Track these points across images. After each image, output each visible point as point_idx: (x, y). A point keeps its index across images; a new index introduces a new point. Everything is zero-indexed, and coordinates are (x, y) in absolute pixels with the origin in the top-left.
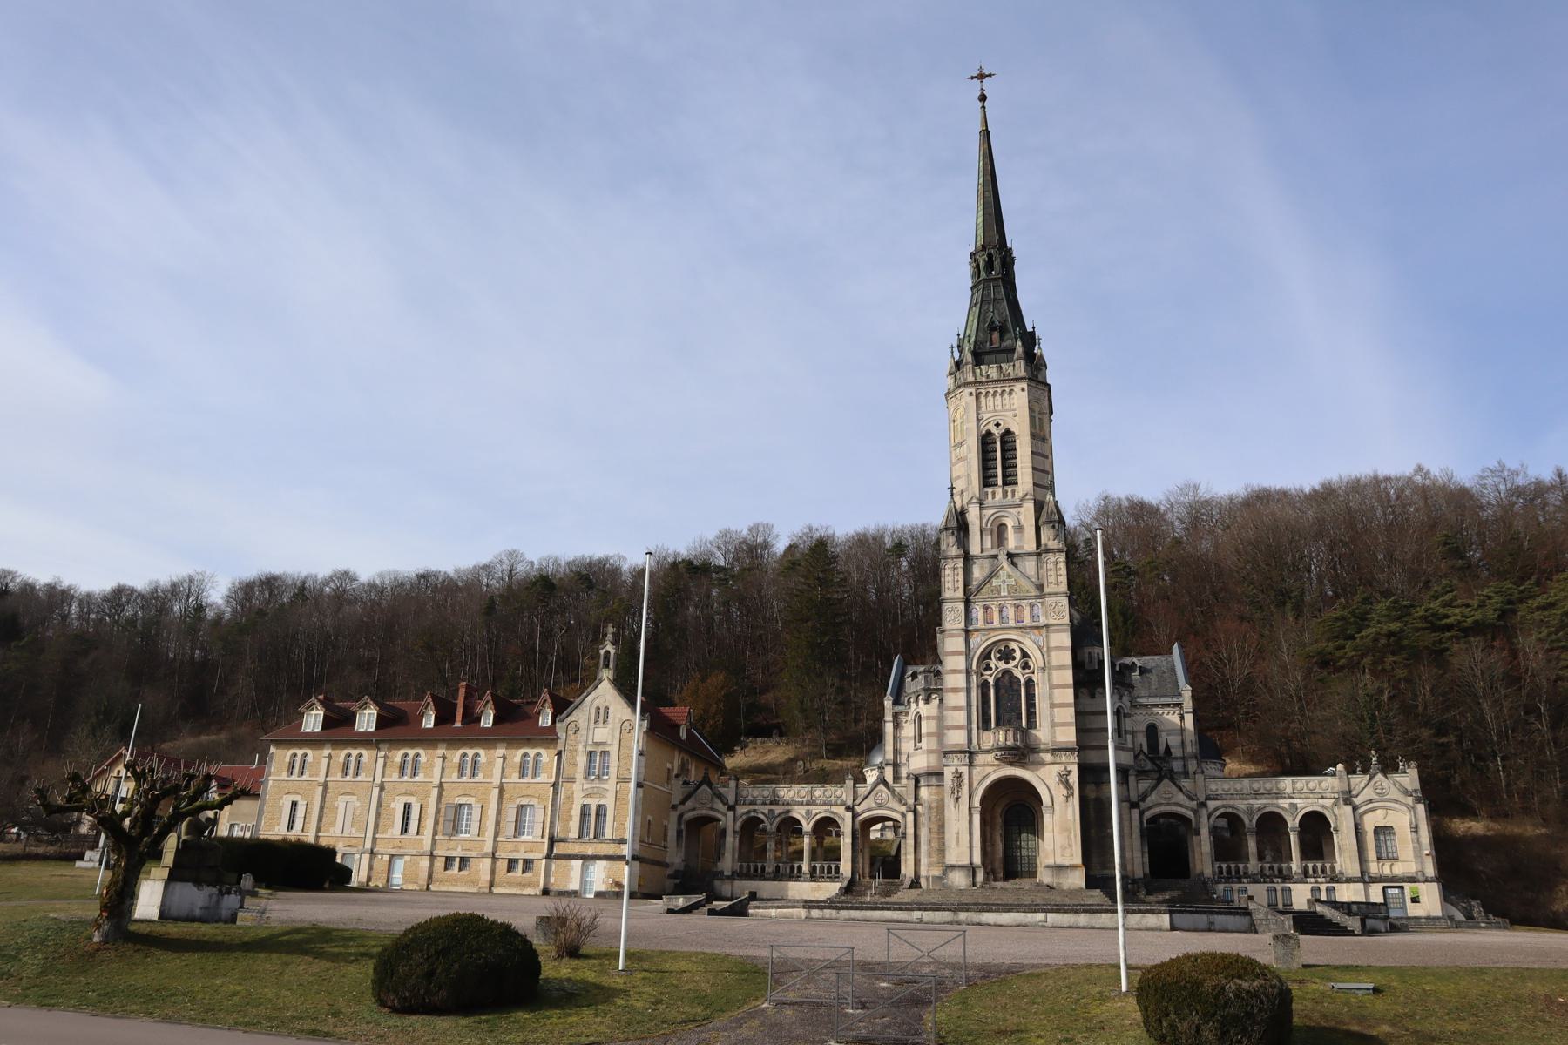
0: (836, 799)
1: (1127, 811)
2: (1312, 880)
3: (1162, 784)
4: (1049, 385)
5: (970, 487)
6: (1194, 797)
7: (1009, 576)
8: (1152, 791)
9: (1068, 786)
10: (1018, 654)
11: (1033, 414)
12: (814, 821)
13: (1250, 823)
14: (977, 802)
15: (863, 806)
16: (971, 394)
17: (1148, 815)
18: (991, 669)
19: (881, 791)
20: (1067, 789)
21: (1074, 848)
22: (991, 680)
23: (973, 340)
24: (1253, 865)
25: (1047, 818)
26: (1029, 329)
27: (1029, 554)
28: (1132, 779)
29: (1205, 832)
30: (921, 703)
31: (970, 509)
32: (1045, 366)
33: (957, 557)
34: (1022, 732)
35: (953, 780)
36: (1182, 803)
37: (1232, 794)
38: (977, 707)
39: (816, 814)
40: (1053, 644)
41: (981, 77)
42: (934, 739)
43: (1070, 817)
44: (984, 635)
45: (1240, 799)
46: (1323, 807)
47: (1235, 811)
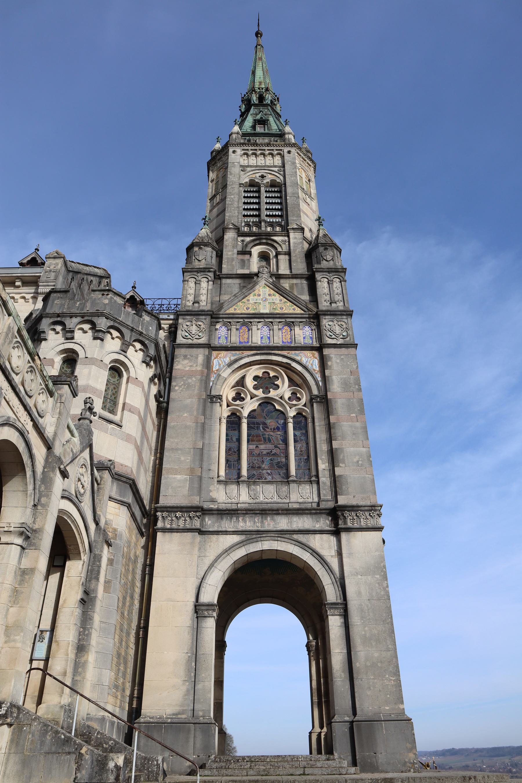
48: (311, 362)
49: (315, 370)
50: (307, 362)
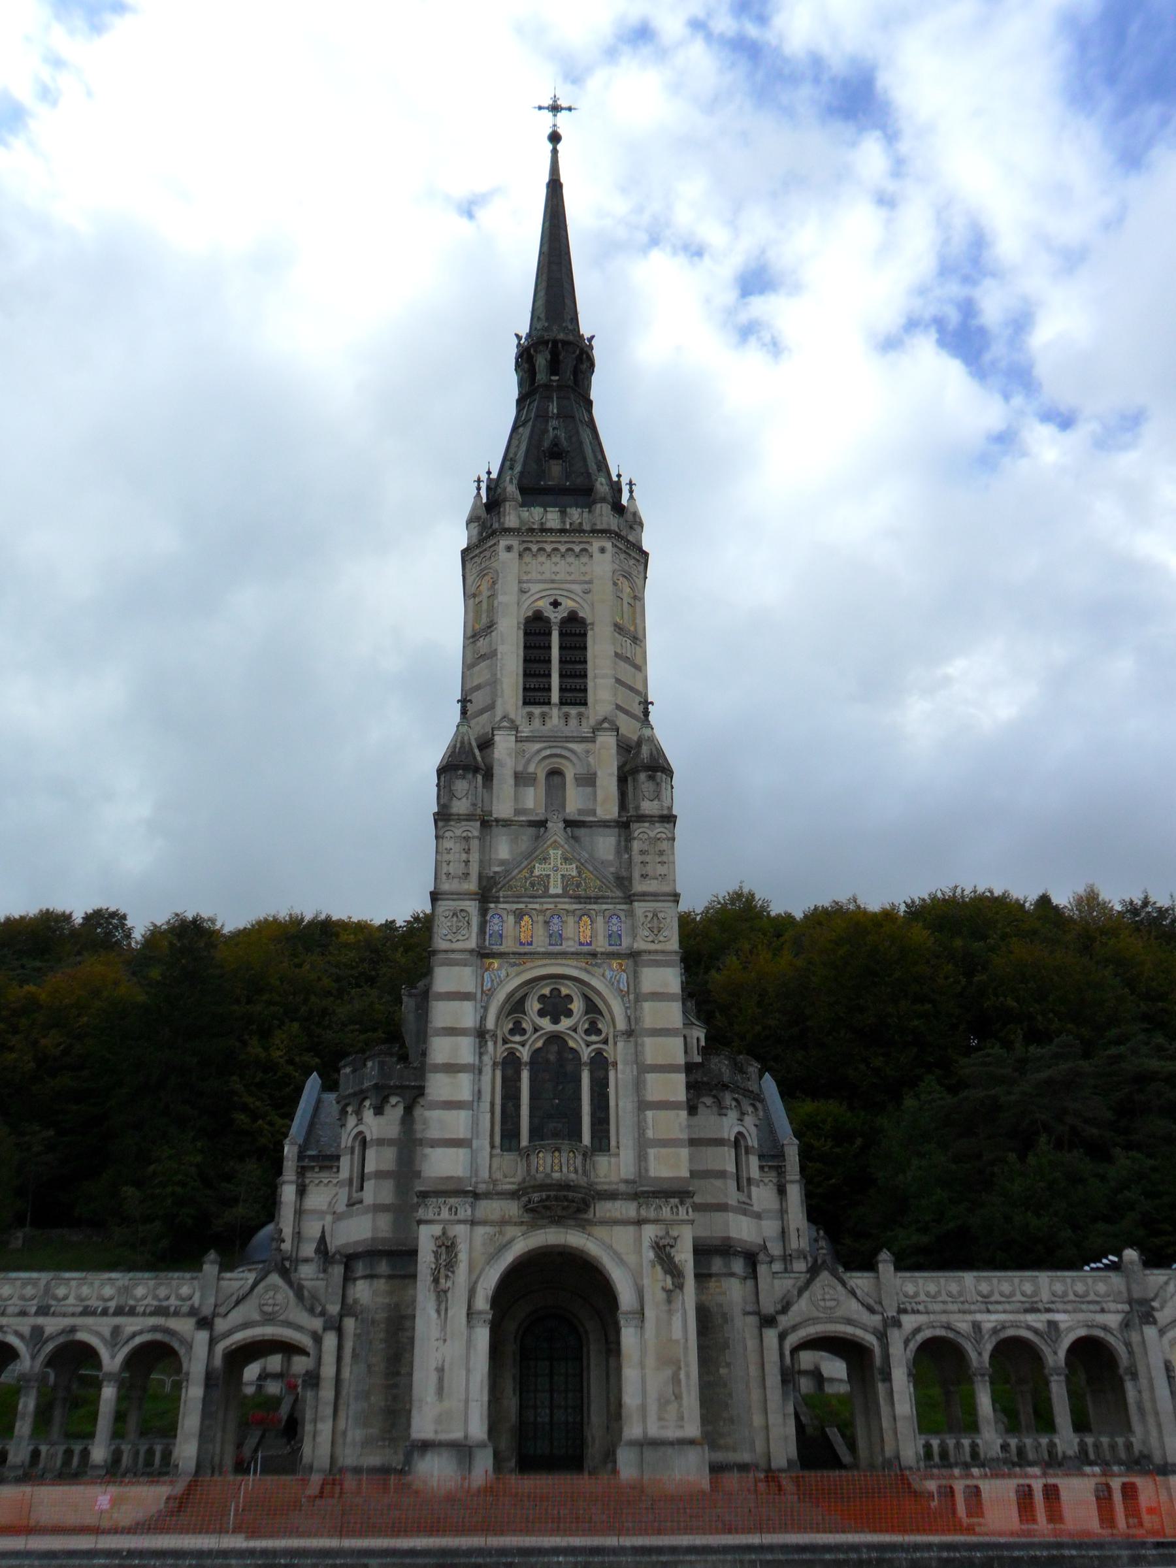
0: (179, 1303)
1: (756, 1331)
2: (1097, 1469)
3: (818, 1279)
4: (646, 554)
5: (499, 702)
6: (877, 1307)
7: (566, 860)
8: (800, 1292)
9: (672, 1269)
10: (577, 1006)
11: (621, 595)
12: (126, 1350)
13: (980, 1357)
14: (482, 1303)
15: (236, 1317)
16: (509, 549)
17: (792, 1340)
18: (523, 1032)
19: (275, 1288)
20: (673, 1276)
21: (685, 1402)
22: (525, 1054)
23: (518, 468)
24: (990, 1438)
25: (628, 1337)
26: (615, 479)
27: (604, 824)
28: (762, 1269)
29: (900, 1375)
30: (368, 1114)
31: (497, 738)
32: (641, 525)
33: (469, 818)
34: (585, 1155)
35: (435, 1253)
36: (855, 1316)
37: (944, 1302)
38: (492, 1104)
39: (134, 1335)
40: (647, 986)
41: (555, 108)
42: (388, 1186)
43: (677, 1334)
44: (515, 965)
45: (960, 1312)
46: (1105, 1328)
47: (951, 1335)
48: (617, 977)
49: (622, 991)
50: (611, 978)
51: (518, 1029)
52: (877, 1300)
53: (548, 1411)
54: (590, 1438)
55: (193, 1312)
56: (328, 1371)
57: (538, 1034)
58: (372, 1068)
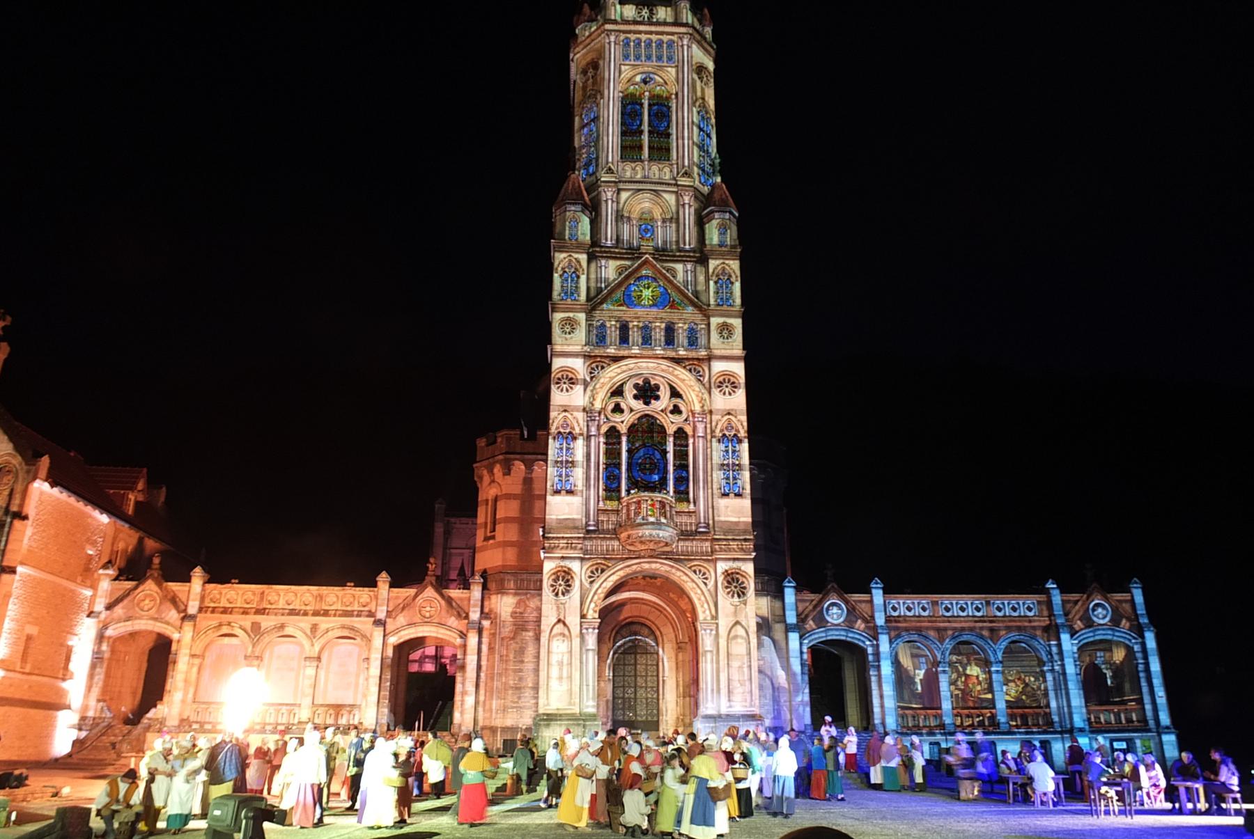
10: (664, 393)
18: (622, 411)
22: (623, 429)
51: (618, 409)
52: (870, 614)
53: (633, 690)
54: (664, 709)
55: (371, 614)
56: (471, 660)
57: (633, 413)
58: (501, 442)
